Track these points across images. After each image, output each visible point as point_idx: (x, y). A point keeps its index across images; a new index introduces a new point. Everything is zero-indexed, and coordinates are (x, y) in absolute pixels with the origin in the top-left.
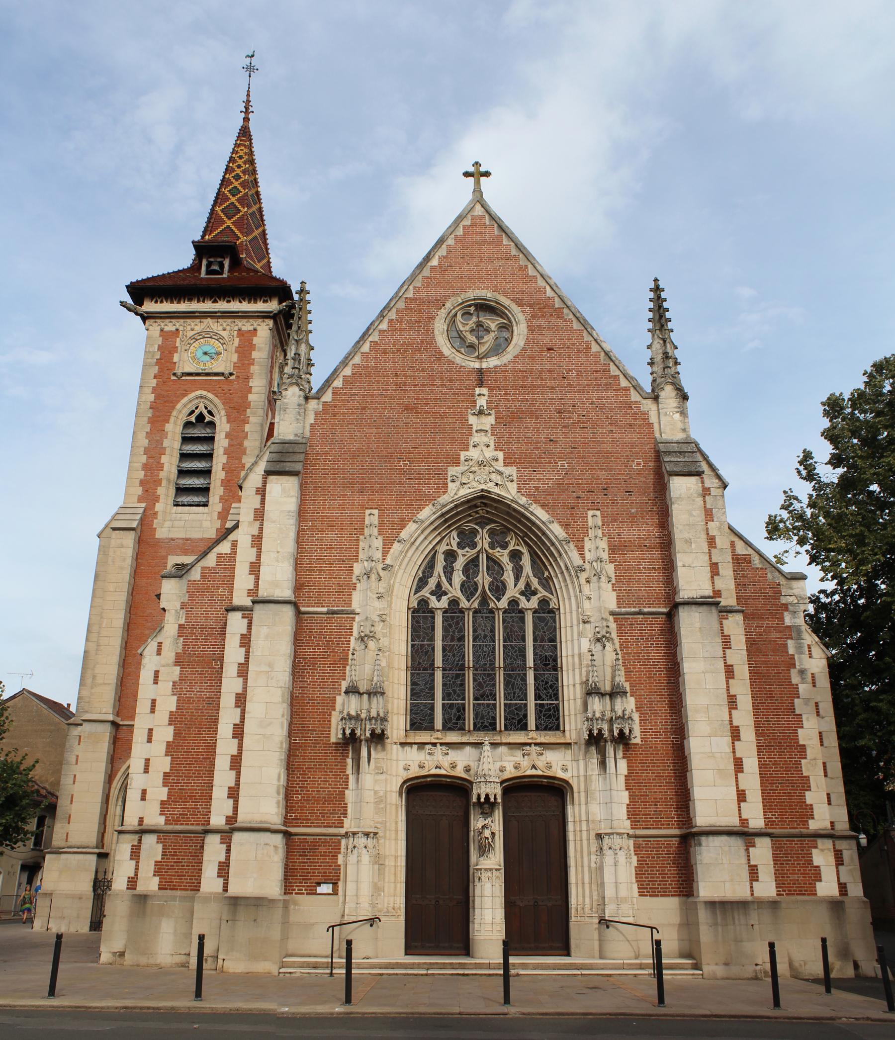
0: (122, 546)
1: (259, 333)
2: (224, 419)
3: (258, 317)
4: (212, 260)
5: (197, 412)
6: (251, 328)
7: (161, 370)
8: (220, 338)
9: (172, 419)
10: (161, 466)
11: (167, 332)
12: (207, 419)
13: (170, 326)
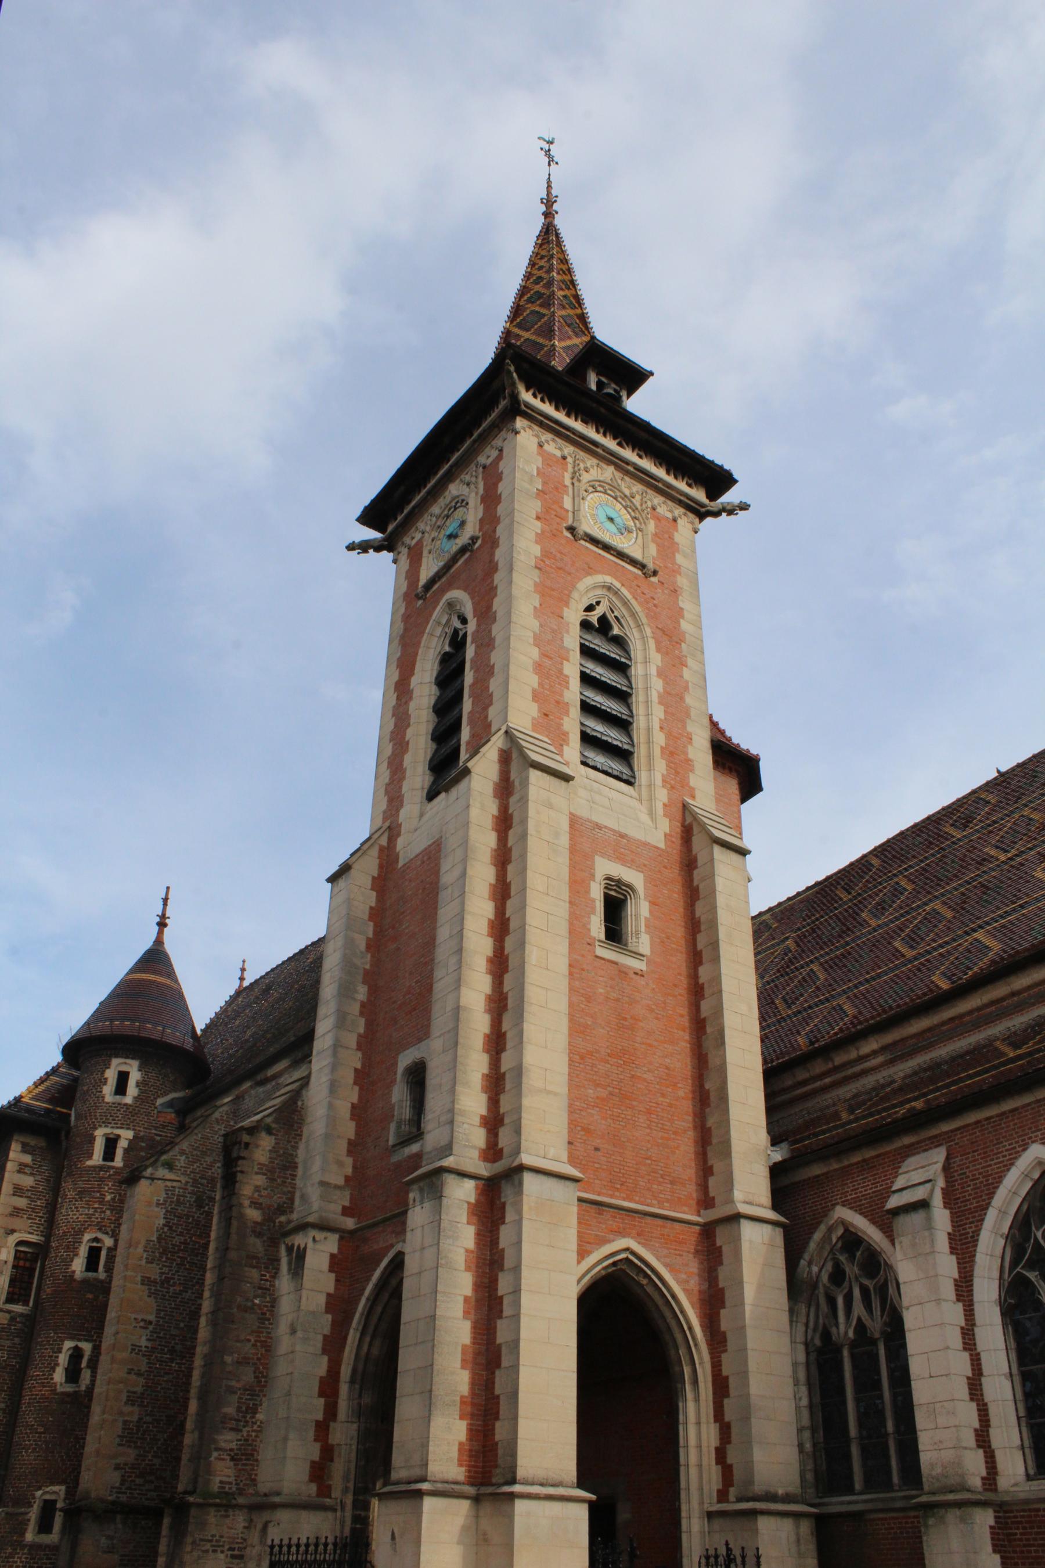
0: (550, 806)
1: (680, 527)
2: (652, 643)
3: (680, 503)
4: (603, 379)
5: (599, 611)
6: (669, 515)
8: (630, 507)
9: (572, 603)
10: (565, 681)
11: (549, 454)
12: (616, 631)
13: (554, 447)
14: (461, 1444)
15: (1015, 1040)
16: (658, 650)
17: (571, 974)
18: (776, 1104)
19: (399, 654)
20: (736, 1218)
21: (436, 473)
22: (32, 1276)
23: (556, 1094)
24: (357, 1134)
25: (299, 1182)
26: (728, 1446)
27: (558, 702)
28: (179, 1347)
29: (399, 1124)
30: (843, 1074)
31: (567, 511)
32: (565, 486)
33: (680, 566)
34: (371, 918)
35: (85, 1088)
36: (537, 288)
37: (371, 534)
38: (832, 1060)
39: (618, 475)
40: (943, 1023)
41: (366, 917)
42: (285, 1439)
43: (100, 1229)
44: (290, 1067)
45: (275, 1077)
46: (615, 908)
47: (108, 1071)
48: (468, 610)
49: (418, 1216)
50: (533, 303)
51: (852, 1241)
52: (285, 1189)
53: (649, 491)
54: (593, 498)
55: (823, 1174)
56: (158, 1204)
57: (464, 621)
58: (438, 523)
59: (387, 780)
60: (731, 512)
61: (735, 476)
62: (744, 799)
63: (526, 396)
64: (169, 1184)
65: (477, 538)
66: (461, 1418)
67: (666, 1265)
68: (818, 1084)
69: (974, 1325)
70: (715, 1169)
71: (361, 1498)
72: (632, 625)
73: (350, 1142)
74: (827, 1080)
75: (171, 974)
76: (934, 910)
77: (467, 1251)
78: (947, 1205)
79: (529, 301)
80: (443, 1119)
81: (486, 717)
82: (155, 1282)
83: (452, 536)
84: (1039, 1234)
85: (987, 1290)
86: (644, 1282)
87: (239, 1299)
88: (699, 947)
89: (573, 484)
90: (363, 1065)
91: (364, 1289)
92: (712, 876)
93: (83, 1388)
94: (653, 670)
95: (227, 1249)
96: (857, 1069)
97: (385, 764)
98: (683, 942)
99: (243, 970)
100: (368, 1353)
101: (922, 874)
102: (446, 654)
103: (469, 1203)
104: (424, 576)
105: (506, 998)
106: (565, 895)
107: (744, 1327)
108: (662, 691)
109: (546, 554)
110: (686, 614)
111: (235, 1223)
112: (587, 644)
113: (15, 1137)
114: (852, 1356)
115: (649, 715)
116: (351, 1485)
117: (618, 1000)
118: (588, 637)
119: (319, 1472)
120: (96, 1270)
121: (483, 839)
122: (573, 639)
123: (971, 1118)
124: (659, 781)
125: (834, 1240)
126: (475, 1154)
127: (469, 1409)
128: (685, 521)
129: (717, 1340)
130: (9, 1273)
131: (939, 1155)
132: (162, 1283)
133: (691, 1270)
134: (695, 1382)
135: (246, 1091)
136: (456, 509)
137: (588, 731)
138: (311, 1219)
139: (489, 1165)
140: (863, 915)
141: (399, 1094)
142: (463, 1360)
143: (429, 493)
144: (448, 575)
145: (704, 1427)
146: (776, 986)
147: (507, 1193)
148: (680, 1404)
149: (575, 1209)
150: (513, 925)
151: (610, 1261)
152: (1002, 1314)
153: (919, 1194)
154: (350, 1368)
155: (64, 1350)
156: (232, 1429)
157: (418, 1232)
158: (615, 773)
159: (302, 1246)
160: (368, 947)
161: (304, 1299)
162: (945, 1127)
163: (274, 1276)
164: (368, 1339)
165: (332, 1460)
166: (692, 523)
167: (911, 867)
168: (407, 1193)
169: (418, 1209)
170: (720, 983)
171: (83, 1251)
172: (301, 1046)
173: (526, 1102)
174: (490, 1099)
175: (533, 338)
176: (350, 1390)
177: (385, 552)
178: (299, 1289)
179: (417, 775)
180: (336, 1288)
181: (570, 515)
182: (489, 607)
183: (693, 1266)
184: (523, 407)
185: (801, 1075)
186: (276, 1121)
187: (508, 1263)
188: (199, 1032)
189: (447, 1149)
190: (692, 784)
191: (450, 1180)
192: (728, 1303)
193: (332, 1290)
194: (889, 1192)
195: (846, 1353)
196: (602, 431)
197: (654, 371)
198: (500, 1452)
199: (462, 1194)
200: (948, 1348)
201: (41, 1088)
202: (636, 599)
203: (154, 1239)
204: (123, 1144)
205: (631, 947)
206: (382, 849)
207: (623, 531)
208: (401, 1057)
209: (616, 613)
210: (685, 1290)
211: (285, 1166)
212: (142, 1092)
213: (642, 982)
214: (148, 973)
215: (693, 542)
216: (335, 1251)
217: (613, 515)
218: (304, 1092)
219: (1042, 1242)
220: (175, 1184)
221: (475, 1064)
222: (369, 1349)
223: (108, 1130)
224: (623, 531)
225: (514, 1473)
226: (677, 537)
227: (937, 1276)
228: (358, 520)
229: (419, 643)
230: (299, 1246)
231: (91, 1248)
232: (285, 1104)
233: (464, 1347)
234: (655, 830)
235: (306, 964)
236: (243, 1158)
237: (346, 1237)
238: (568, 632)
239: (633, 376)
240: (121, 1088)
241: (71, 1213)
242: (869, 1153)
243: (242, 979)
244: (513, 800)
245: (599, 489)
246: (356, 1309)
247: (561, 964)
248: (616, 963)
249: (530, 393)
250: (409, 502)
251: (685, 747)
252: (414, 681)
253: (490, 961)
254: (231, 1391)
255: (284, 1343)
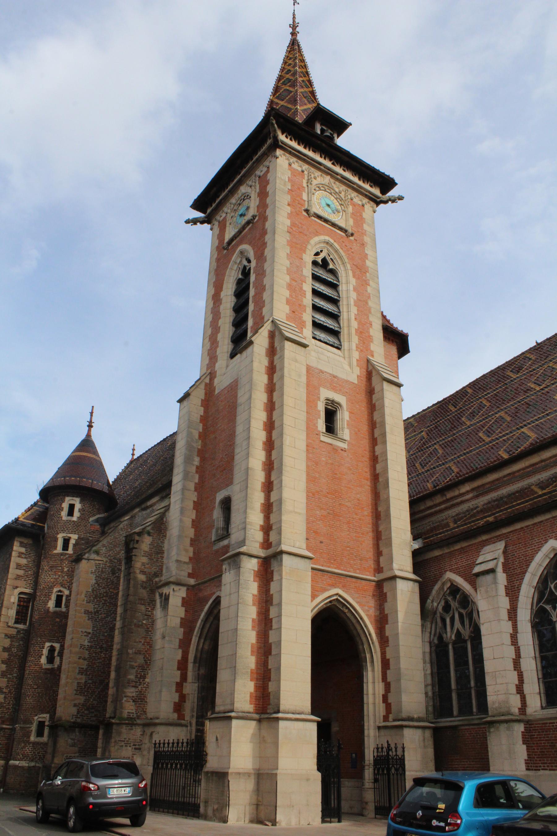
0: (296, 361)
1: (366, 209)
2: (350, 273)
3: (366, 196)
6: (360, 203)
7: (293, 200)
8: (339, 199)
9: (308, 252)
12: (331, 266)
13: (297, 165)
14: (251, 693)
15: (542, 485)
16: (354, 276)
17: (307, 450)
18: (416, 518)
19: (214, 280)
20: (394, 578)
21: (233, 181)
22: (27, 610)
23: (300, 514)
24: (195, 535)
25: (165, 560)
26: (389, 694)
27: (300, 305)
28: (104, 646)
29: (217, 530)
30: (451, 503)
31: (305, 201)
32: (304, 187)
33: (366, 231)
34: (201, 421)
35: (52, 513)
36: (287, 76)
37: (198, 215)
38: (446, 496)
39: (332, 181)
40: (504, 477)
41: (199, 421)
42: (161, 691)
43: (62, 586)
44: (159, 500)
45: (151, 506)
46: (330, 415)
47: (63, 504)
48: (251, 256)
49: (228, 577)
50: (285, 85)
51: (455, 590)
52: (158, 564)
53: (349, 190)
54: (318, 194)
55: (440, 555)
56: (92, 573)
57: (249, 261)
58: (235, 208)
59: (209, 348)
60: (393, 201)
61: (396, 181)
62: (400, 357)
63: (282, 137)
64: (97, 562)
65: (256, 216)
66: (251, 680)
67: (358, 602)
68: (438, 508)
69: (517, 632)
70: (383, 553)
71: (200, 720)
72: (339, 262)
73: (192, 540)
74: (443, 506)
75: (95, 452)
76: (501, 417)
77: (253, 595)
78: (504, 571)
79: (284, 84)
80: (240, 527)
81: (262, 313)
82: (91, 612)
83: (242, 215)
84: (552, 586)
85: (525, 615)
86: (346, 611)
87: (135, 621)
88: (376, 436)
89: (308, 186)
90: (198, 499)
91: (200, 615)
92: (383, 398)
93: (56, 666)
94: (351, 288)
95: (128, 595)
96: (459, 500)
97: (208, 339)
98: (367, 433)
99: (134, 450)
100: (203, 648)
101: (494, 397)
102: (239, 279)
103: (254, 571)
104: (227, 237)
105: (273, 463)
106: (304, 409)
107: (398, 634)
108: (356, 298)
109: (293, 225)
110: (369, 257)
111: (132, 582)
112: (316, 273)
113: (16, 539)
114: (454, 648)
115: (349, 312)
116: (195, 714)
117: (332, 464)
118: (316, 269)
119: (178, 707)
120: (60, 607)
121: (260, 379)
122: (308, 271)
123: (518, 526)
124: (354, 347)
125: (445, 589)
126: (258, 545)
127: (255, 676)
128: (369, 206)
129: (384, 641)
130: (15, 609)
131: (501, 545)
132: (95, 613)
133: (370, 605)
134: (372, 661)
135: (136, 514)
136: (244, 200)
137: (316, 320)
138: (172, 580)
139: (265, 551)
140: (463, 419)
141: (217, 514)
142: (252, 651)
143: (229, 191)
144: (240, 236)
145: (376, 684)
146: (416, 457)
147: (274, 565)
148: (365, 673)
149: (310, 574)
150: (276, 425)
151: (328, 600)
152: (532, 627)
153: (490, 565)
154: (193, 655)
155: (45, 647)
156: (133, 686)
157: (228, 586)
158: (331, 343)
159: (167, 594)
160: (200, 437)
161: (169, 620)
162: (505, 531)
163: (153, 609)
164: (202, 641)
165: (185, 702)
166: (372, 207)
167: (489, 393)
168: (222, 565)
169: (228, 574)
170: (386, 455)
171: (54, 597)
172: (165, 489)
173: (284, 518)
174: (265, 516)
175: (286, 104)
176: (194, 667)
177: (206, 224)
178: (166, 616)
179: (225, 345)
180: (185, 615)
181: (306, 203)
182: (263, 253)
183: (372, 603)
184: (280, 143)
185: (429, 503)
186: (152, 529)
187: (275, 601)
188: (111, 483)
189: (243, 543)
190: (372, 349)
191: (244, 559)
192: (389, 622)
193: (183, 616)
194: (474, 564)
195: (450, 647)
196: (323, 156)
197: (352, 123)
198: (271, 697)
199: (250, 566)
200: (503, 644)
201: (29, 513)
202: (342, 249)
203: (90, 590)
204: (72, 542)
205: (339, 435)
206: (206, 385)
207: (335, 211)
208: (218, 494)
209: (331, 257)
210: (367, 615)
211: (158, 552)
212: (82, 514)
213: (345, 454)
214: (83, 452)
215: (373, 218)
216: (185, 596)
217: (329, 203)
218: (167, 513)
219: (554, 590)
220: (100, 562)
221: (257, 498)
222: (203, 646)
223: (64, 535)
224: (335, 211)
225: (279, 707)
226: (364, 215)
227: (498, 607)
228: (191, 207)
229: (225, 274)
230: (166, 594)
231: (58, 596)
232: (157, 520)
233: (252, 644)
234: (352, 374)
235: (167, 446)
236: (136, 548)
237: (190, 588)
238: (305, 267)
239: (341, 126)
240: (71, 512)
241: (47, 577)
242: (464, 544)
243: (133, 455)
244: (276, 358)
245: (322, 188)
246: (196, 626)
247: (302, 444)
248: (331, 444)
249: (284, 135)
250: (219, 197)
251: (368, 329)
252: (223, 294)
253: (264, 443)
254: (132, 667)
255: (159, 644)
